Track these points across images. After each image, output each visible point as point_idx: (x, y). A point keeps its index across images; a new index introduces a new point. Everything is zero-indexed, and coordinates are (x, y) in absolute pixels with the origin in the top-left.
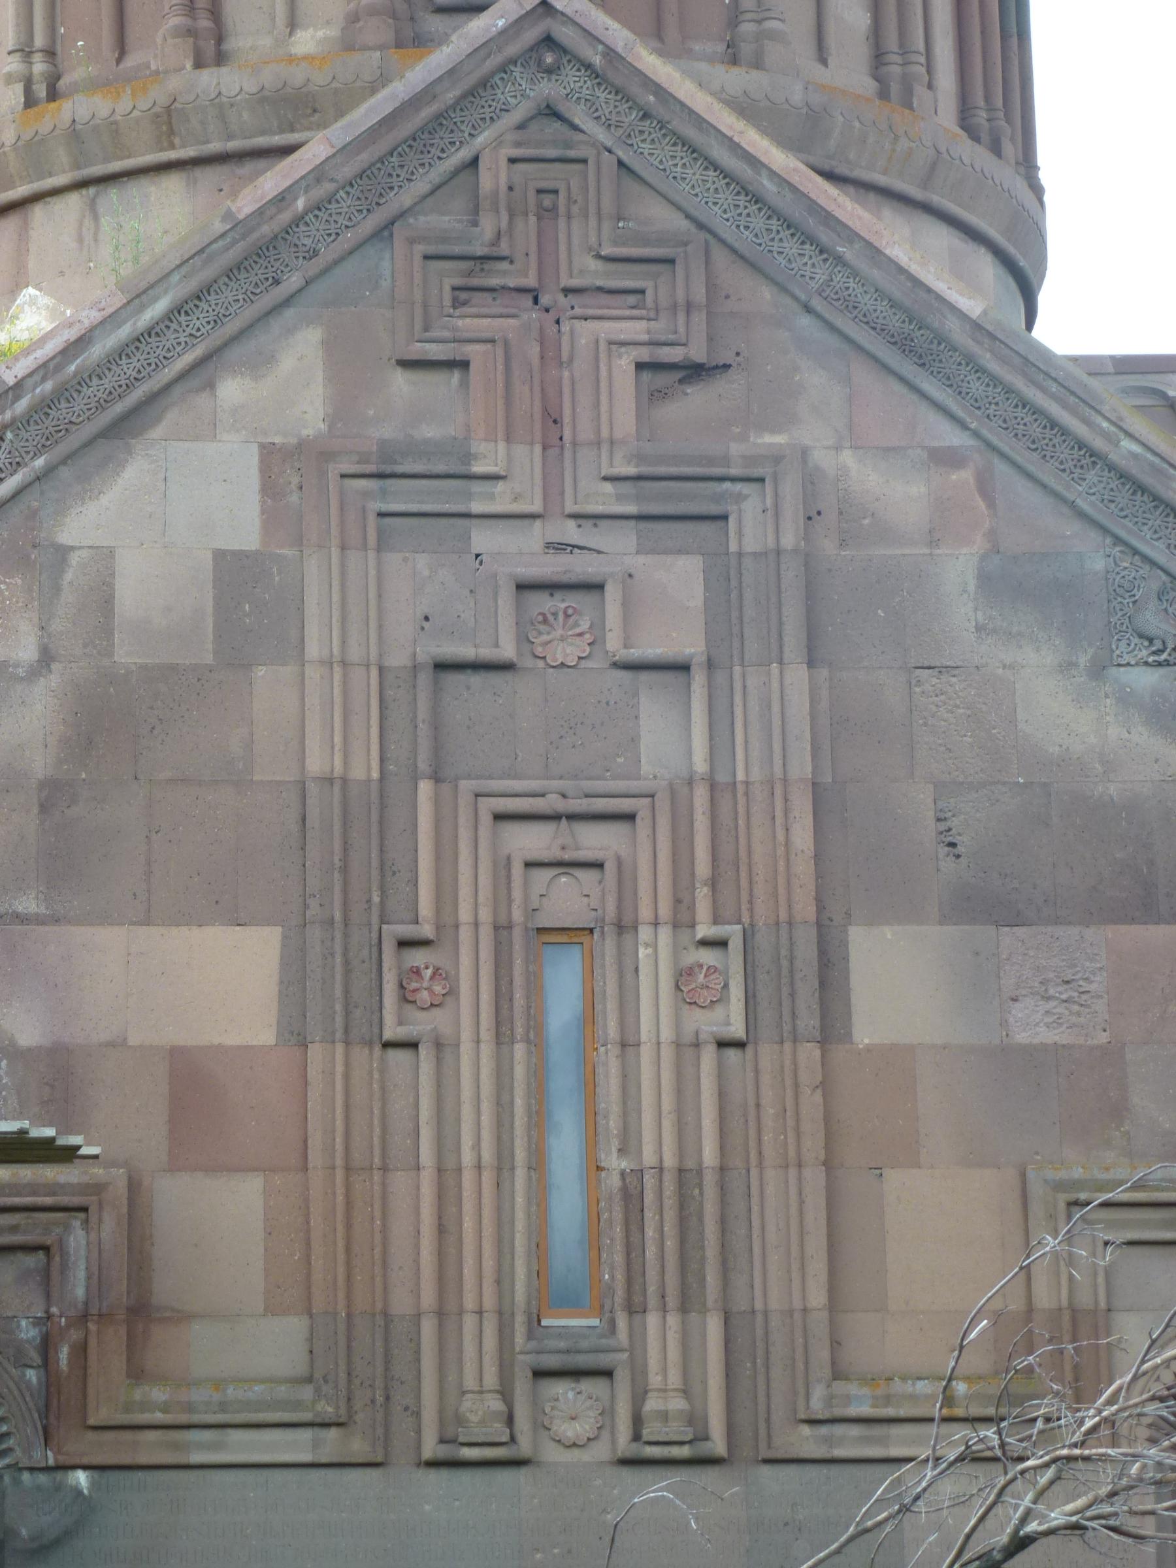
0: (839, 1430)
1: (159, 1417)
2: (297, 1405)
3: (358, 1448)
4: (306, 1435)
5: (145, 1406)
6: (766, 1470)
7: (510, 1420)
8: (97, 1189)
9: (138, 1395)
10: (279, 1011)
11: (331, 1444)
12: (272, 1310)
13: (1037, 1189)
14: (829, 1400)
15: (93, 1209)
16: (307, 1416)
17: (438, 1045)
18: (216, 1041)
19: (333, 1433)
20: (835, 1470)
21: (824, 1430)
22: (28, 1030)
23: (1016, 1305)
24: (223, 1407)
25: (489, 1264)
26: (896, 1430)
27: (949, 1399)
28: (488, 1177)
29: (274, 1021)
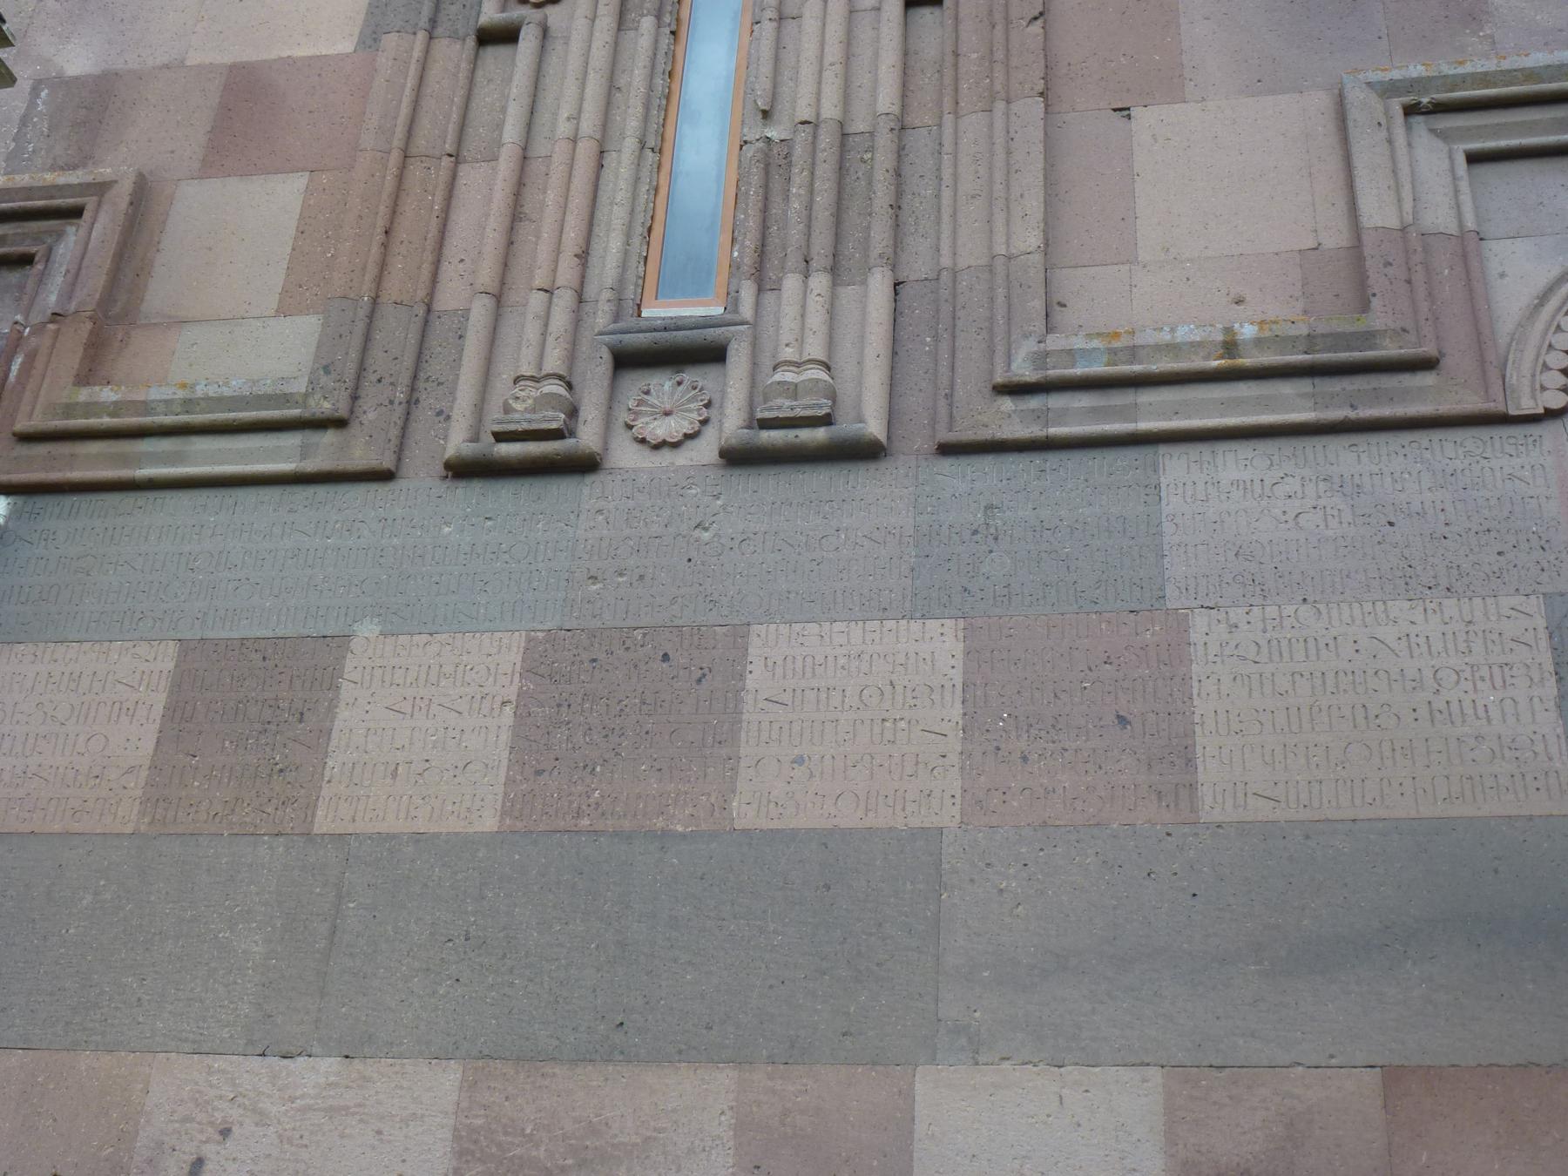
0: (1056, 401)
1: (106, 421)
2: (286, 399)
3: (360, 455)
4: (291, 440)
5: (91, 408)
6: (948, 464)
7: (573, 413)
8: (101, 189)
9: (83, 395)
10: (366, 20)
11: (324, 452)
12: (283, 311)
13: (1357, 96)
14: (1041, 358)
15: (87, 215)
16: (294, 412)
17: (545, 31)
18: (285, 54)
19: (329, 437)
20: (1053, 459)
21: (1034, 402)
22: (78, 61)
23: (1335, 237)
24: (188, 404)
25: (573, 237)
26: (1147, 397)
27: (1230, 346)
28: (586, 150)
29: (357, 31)
